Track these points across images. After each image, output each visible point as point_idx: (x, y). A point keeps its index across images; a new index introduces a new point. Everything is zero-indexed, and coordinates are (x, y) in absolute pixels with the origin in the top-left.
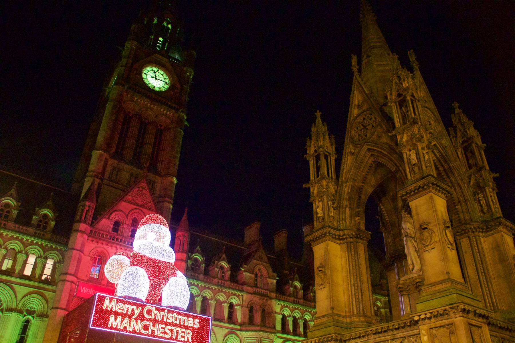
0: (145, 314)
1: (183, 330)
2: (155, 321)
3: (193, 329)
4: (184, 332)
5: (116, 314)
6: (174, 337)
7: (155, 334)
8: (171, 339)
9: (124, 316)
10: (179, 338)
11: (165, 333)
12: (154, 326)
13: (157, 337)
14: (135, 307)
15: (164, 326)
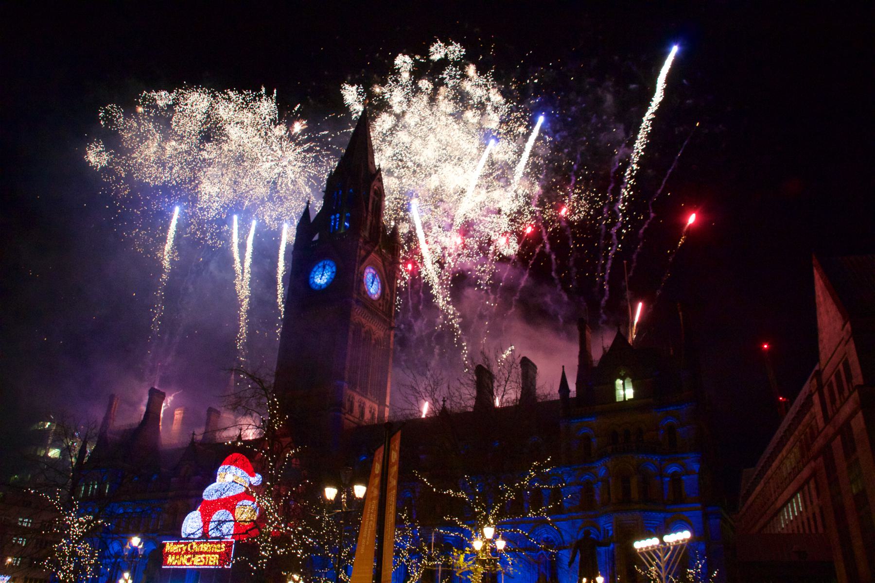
0: (189, 549)
1: (213, 555)
2: (195, 554)
3: (219, 554)
4: (213, 558)
5: (172, 554)
6: (206, 564)
7: (194, 564)
8: (204, 565)
9: (176, 554)
10: (211, 563)
11: (201, 561)
12: (194, 557)
13: (195, 565)
14: (183, 545)
15: (200, 556)
